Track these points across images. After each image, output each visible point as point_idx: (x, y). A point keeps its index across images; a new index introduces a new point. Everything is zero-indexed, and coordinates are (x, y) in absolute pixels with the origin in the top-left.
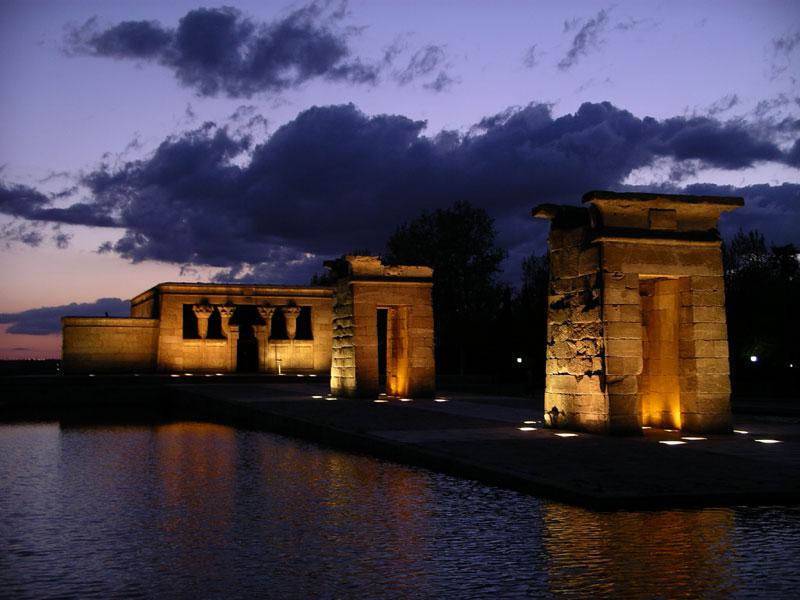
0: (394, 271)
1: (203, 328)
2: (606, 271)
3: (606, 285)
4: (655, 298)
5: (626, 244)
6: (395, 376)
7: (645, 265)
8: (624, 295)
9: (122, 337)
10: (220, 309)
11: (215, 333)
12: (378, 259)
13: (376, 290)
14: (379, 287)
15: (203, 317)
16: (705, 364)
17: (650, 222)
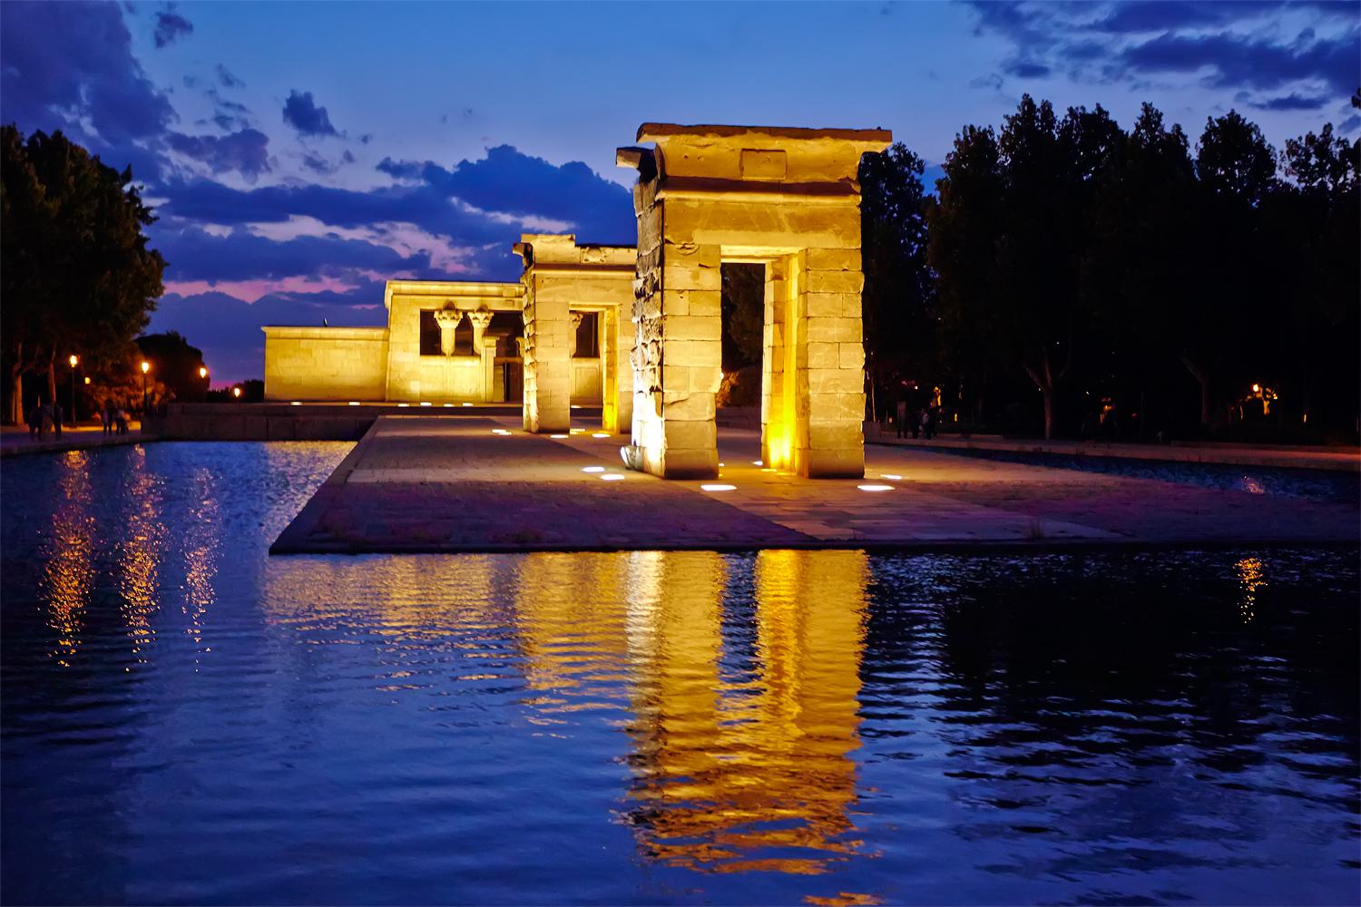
0: (594, 257)
1: (448, 341)
2: (668, 242)
3: (667, 261)
4: (789, 281)
5: (699, 200)
6: (613, 405)
7: (732, 232)
8: (695, 276)
9: (341, 353)
10: (471, 315)
11: (465, 346)
12: (571, 239)
13: (565, 283)
14: (573, 279)
15: (448, 327)
16: (822, 378)
17: (742, 169)
